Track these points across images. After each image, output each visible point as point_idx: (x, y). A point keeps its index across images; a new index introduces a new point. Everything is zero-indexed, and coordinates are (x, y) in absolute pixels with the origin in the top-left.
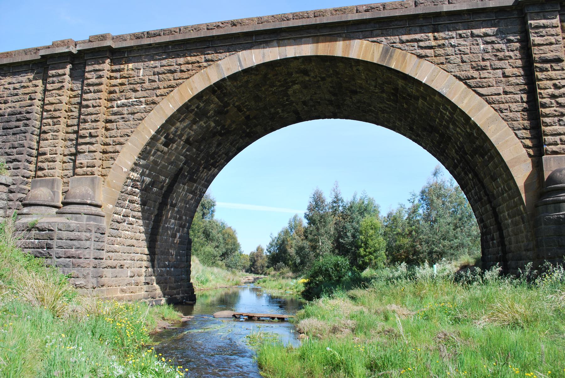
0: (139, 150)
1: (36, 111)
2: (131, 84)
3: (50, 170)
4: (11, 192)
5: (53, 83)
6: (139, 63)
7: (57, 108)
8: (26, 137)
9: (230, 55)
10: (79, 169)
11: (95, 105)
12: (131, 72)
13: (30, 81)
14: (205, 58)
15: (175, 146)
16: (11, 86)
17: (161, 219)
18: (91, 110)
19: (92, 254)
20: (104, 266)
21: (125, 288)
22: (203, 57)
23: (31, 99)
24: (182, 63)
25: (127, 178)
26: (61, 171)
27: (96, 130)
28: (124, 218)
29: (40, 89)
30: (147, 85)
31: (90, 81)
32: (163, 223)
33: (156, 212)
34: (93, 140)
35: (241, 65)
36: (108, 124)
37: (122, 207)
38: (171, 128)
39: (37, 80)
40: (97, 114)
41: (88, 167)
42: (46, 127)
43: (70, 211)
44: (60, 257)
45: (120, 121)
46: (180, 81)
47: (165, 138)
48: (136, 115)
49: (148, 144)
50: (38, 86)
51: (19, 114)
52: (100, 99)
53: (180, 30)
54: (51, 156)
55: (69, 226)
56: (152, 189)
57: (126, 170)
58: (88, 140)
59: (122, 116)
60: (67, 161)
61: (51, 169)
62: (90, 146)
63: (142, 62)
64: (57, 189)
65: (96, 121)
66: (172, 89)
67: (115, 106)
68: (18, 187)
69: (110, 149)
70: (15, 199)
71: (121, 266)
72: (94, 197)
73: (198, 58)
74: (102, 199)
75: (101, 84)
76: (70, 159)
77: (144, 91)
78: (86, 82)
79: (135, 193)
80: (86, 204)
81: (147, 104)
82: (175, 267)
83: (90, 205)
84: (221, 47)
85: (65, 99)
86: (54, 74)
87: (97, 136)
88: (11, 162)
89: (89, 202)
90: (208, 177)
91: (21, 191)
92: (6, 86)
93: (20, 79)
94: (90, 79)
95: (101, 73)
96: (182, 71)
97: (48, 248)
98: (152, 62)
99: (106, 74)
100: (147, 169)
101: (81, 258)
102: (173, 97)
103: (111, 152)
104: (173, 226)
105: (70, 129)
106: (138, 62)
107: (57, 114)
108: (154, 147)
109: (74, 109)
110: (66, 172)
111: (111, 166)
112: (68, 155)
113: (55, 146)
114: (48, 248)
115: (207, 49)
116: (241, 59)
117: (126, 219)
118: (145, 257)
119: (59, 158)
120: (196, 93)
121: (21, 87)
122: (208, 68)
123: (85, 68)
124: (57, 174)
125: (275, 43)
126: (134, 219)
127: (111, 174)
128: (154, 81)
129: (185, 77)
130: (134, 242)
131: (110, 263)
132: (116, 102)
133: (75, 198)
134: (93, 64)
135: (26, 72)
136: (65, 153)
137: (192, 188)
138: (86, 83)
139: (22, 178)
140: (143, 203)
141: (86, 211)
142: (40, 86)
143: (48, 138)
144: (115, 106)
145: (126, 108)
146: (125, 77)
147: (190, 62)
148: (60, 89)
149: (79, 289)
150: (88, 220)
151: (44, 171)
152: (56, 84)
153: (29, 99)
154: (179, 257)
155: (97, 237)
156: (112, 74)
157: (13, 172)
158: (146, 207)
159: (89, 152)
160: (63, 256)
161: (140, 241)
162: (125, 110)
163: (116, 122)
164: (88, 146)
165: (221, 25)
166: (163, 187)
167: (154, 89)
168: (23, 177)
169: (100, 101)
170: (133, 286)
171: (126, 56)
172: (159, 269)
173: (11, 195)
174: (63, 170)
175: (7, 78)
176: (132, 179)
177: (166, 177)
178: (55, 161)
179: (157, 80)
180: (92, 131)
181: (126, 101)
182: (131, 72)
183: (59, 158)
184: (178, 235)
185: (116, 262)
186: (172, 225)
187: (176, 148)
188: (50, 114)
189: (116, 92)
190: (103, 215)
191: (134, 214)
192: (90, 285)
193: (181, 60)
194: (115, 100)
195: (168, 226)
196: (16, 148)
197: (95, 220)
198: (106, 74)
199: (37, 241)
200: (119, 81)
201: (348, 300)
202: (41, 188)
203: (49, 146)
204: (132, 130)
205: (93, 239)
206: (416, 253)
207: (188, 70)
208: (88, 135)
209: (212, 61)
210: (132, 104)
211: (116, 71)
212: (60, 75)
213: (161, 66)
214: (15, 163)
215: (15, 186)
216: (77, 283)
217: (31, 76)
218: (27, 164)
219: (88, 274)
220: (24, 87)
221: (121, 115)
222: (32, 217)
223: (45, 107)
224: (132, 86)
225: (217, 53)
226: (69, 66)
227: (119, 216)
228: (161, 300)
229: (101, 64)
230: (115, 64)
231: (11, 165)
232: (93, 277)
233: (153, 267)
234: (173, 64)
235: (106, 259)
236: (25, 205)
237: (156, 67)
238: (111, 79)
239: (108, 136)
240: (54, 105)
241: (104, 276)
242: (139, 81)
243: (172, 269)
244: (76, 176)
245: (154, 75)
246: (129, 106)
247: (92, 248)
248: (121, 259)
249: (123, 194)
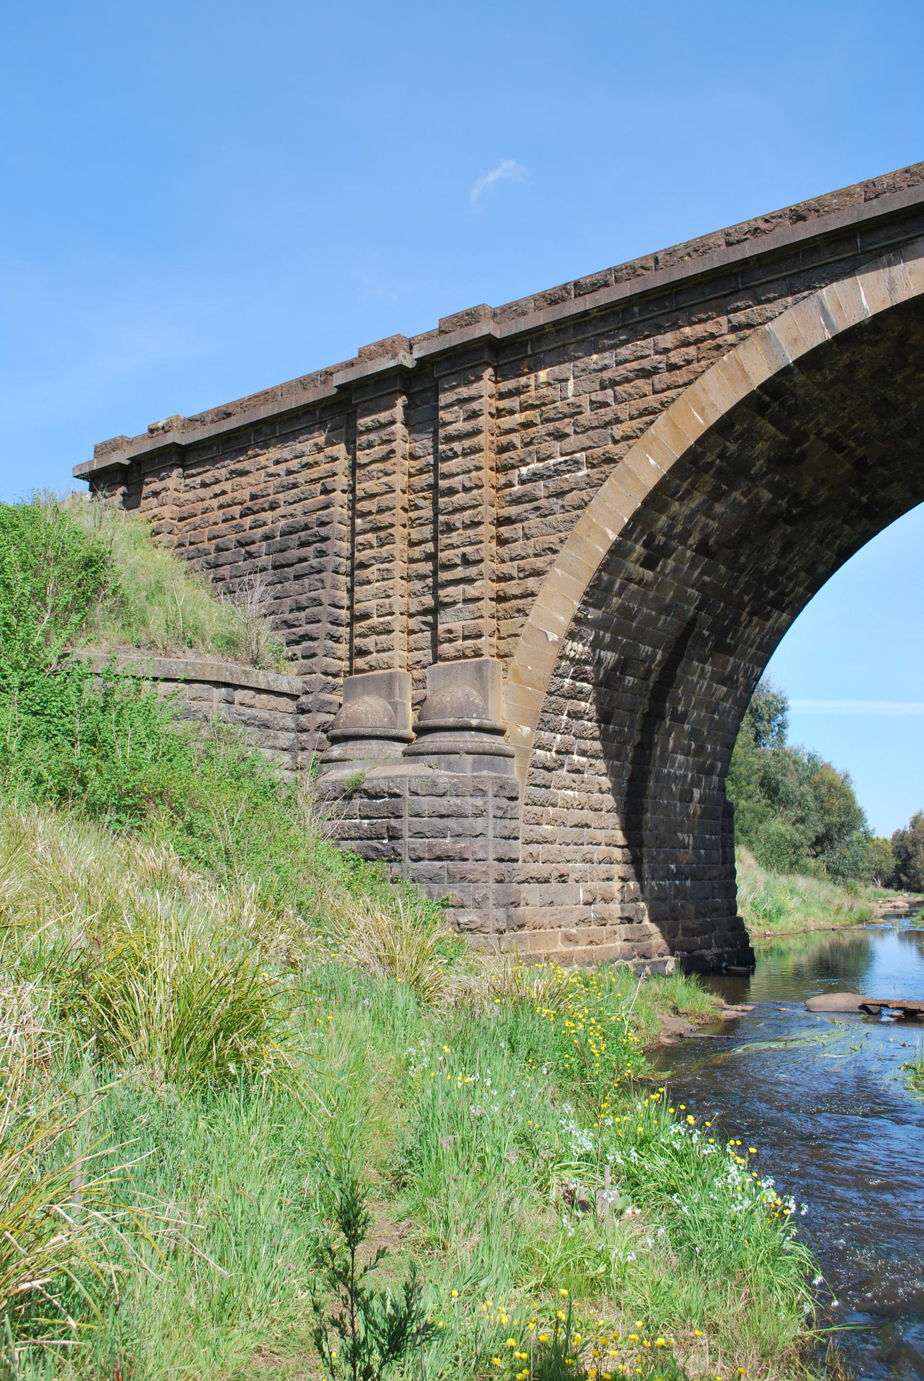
0: (583, 586)
1: (338, 518)
2: (548, 420)
3: (382, 654)
4: (303, 711)
5: (370, 446)
6: (562, 366)
7: (384, 504)
8: (323, 581)
9: (796, 303)
10: (446, 645)
11: (468, 485)
12: (544, 391)
13: (320, 450)
14: (729, 321)
15: (671, 563)
16: (282, 468)
17: (650, 755)
18: (460, 499)
19: (491, 850)
20: (522, 878)
21: (574, 931)
22: (723, 320)
23: (326, 491)
24: (669, 346)
25: (561, 658)
26: (406, 654)
27: (476, 547)
28: (561, 757)
29: (343, 464)
30: (587, 416)
31: (451, 430)
32: (657, 764)
33: (637, 738)
34: (472, 571)
35: (829, 325)
36: (502, 529)
37: (552, 731)
38: (658, 520)
39: (333, 444)
40: (474, 507)
41: (465, 638)
42: (363, 553)
43: (432, 747)
44: (419, 859)
45: (531, 516)
46: (670, 394)
47: (645, 545)
48: (568, 496)
49: (605, 566)
50: (337, 459)
51: (303, 530)
52: (478, 469)
53: (656, 260)
54: (382, 619)
55: (435, 784)
56: (621, 680)
57: (556, 637)
58: (459, 572)
59: (535, 504)
60: (417, 628)
61: (384, 651)
62: (467, 587)
63: (571, 360)
64: (401, 696)
65: (475, 524)
66: (652, 417)
67: (516, 482)
68: (316, 699)
69: (512, 588)
70: (312, 728)
71: (562, 878)
72: (485, 711)
73: (710, 327)
74: (504, 714)
75: (477, 432)
76: (424, 623)
77: (583, 432)
78: (442, 433)
79: (581, 692)
80: (470, 728)
81: (593, 466)
82: (695, 878)
83: (479, 729)
84: (770, 286)
85: (399, 481)
86: (370, 424)
87: (482, 561)
88: (297, 643)
89: (474, 722)
90: (765, 636)
91: (324, 707)
92: (271, 470)
93: (299, 447)
94: (451, 423)
95: (475, 405)
96: (672, 367)
97: (391, 838)
98: (595, 357)
99: (487, 404)
100: (606, 630)
101: (467, 860)
102: (655, 438)
103: (515, 597)
104: (682, 772)
105: (417, 552)
106: (559, 363)
107: (386, 518)
108: (620, 572)
110: (418, 656)
111: (519, 631)
112: (419, 613)
113: (388, 596)
114: (391, 838)
115: (733, 298)
116: (828, 306)
117: (566, 758)
118: (618, 854)
119: (399, 622)
120: (713, 418)
121: (303, 466)
122: (740, 348)
123: (437, 400)
124: (397, 662)
126: (584, 759)
127: (521, 649)
128: (606, 405)
129: (681, 382)
130: (587, 816)
131: (534, 869)
132: (516, 472)
134: (454, 387)
135: (309, 430)
136: (412, 611)
137: (725, 669)
138: (444, 434)
139: (323, 677)
140: (604, 718)
141: (470, 746)
142: (342, 459)
143: (371, 577)
144: (516, 482)
145: (542, 483)
146: (533, 407)
147: (692, 339)
148: (385, 458)
149: (467, 935)
150: (476, 767)
151: (369, 658)
152: (377, 448)
153: (322, 493)
154: (702, 852)
155: (499, 808)
156: (503, 404)
157: (302, 665)
158: (611, 727)
159: (466, 601)
160: (427, 855)
161: (603, 812)
162: (540, 489)
163: (522, 521)
164: (461, 587)
165: (763, 226)
166: (649, 671)
167: (607, 424)
168: (326, 674)
169: (480, 473)
170: (593, 927)
171: (530, 352)
172: (654, 883)
173: (303, 718)
174: (410, 651)
175: (272, 450)
176: (572, 660)
177: (656, 647)
178: (390, 632)
179: (611, 400)
180: (468, 550)
181: (541, 465)
182: (544, 391)
183: (399, 622)
184: (697, 793)
185: (549, 867)
186: (680, 768)
187: (676, 570)
188: (371, 522)
189: (515, 448)
190: (510, 753)
191: (583, 747)
192: (491, 926)
193: (667, 339)
194: (513, 467)
195: (669, 773)
196: (304, 609)
197: (491, 767)
199: (366, 821)
200: (519, 418)
202: (366, 698)
203: (375, 596)
204: (562, 535)
205: (491, 812)
207: (689, 362)
208: (458, 561)
209: (749, 326)
210: (556, 471)
211: (510, 394)
212: (382, 426)
213: (619, 363)
214: (306, 644)
215: (310, 698)
216: (461, 920)
217: (320, 438)
218: (330, 643)
219: (486, 897)
220: (308, 466)
221: (531, 501)
222: (352, 767)
223: (358, 506)
224: (550, 426)
225: (760, 303)
226: (401, 401)
227: (548, 753)
228: (665, 963)
229: (473, 382)
230: (505, 378)
231: (298, 649)
232: (497, 905)
233: (639, 877)
234: (647, 352)
235: (524, 861)
236: (335, 740)
237: (605, 368)
238: (499, 417)
239: (506, 557)
240: (377, 498)
241: (523, 903)
242: (566, 410)
243: (688, 883)
244: (440, 664)
245: (603, 388)
246: (550, 477)
247: (491, 834)
248: (559, 859)
249: (554, 698)
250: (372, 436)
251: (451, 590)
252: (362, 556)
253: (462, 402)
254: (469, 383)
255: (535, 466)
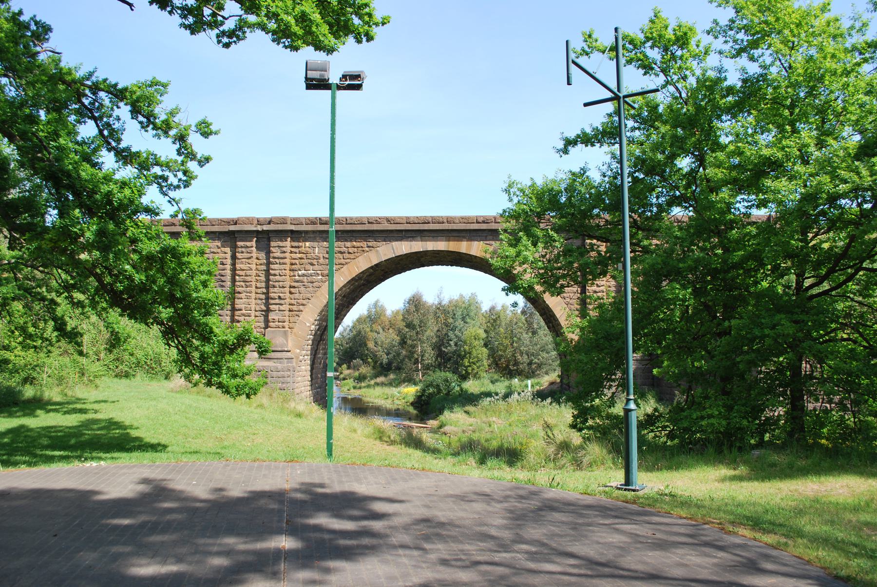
0: (319, 311)
7: (248, 274)
12: (308, 249)
13: (219, 248)
18: (278, 278)
22: (365, 243)
23: (223, 264)
29: (229, 255)
31: (275, 255)
34: (282, 302)
35: (394, 253)
58: (277, 301)
65: (283, 287)
69: (295, 308)
78: (272, 255)
89: (286, 349)
95: (284, 249)
96: (349, 253)
105: (259, 291)
109: (261, 275)
110: (259, 324)
119: (253, 313)
125: (419, 238)
127: (297, 327)
133: (275, 347)
141: (286, 357)
146: (303, 253)
156: (293, 250)
180: (281, 295)
182: (308, 249)
183: (253, 313)
193: (348, 244)
198: (288, 249)
201: (464, 414)
203: (244, 304)
206: (516, 363)
211: (296, 247)
212: (247, 247)
220: (214, 253)
224: (310, 261)
230: (294, 241)
250: (243, 250)
251: (274, 306)
252: (238, 289)
253: (279, 247)
254: (282, 241)
255: (303, 272)
